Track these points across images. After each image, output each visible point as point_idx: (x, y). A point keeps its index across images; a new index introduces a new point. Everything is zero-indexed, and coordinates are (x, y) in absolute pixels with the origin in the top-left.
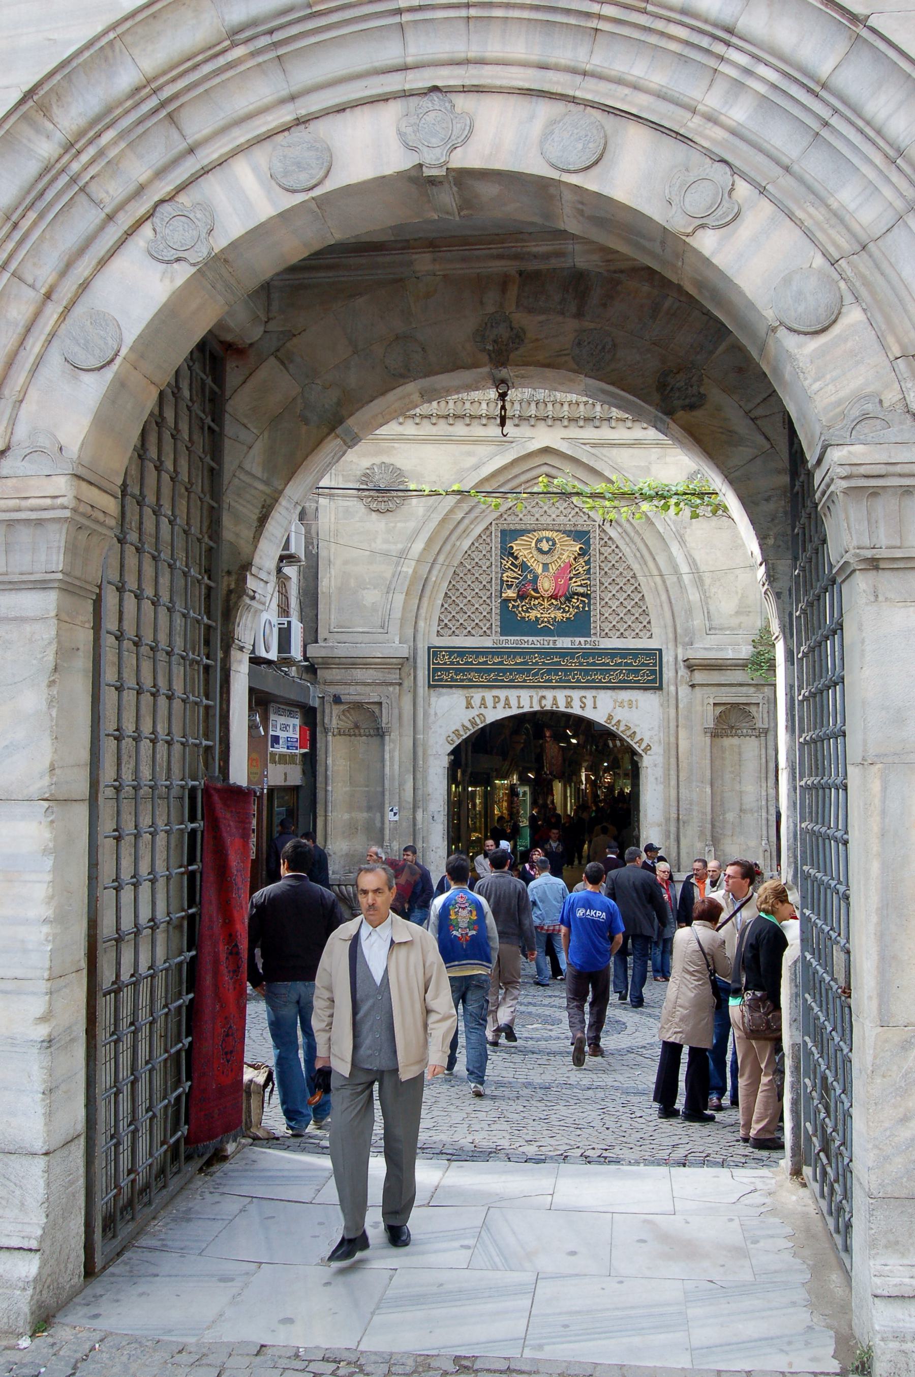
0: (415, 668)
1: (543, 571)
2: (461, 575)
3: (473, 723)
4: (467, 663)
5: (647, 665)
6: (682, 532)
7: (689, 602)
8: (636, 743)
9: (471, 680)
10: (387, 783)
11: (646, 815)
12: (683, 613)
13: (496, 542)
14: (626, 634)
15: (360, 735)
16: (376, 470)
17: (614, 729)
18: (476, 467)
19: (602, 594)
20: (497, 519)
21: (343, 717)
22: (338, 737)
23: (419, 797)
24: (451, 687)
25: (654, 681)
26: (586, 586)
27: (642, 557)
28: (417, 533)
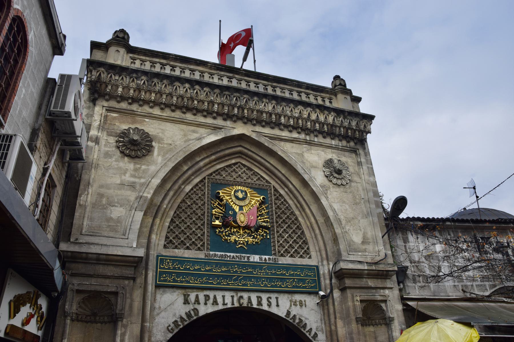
0: (147, 269)
1: (239, 211)
2: (184, 208)
3: (188, 315)
4: (185, 269)
7: (335, 233)
8: (307, 332)
12: (330, 242)
14: (295, 255)
16: (131, 131)
17: (291, 321)
18: (199, 139)
19: (279, 229)
21: (83, 306)
26: (267, 222)
27: (302, 206)
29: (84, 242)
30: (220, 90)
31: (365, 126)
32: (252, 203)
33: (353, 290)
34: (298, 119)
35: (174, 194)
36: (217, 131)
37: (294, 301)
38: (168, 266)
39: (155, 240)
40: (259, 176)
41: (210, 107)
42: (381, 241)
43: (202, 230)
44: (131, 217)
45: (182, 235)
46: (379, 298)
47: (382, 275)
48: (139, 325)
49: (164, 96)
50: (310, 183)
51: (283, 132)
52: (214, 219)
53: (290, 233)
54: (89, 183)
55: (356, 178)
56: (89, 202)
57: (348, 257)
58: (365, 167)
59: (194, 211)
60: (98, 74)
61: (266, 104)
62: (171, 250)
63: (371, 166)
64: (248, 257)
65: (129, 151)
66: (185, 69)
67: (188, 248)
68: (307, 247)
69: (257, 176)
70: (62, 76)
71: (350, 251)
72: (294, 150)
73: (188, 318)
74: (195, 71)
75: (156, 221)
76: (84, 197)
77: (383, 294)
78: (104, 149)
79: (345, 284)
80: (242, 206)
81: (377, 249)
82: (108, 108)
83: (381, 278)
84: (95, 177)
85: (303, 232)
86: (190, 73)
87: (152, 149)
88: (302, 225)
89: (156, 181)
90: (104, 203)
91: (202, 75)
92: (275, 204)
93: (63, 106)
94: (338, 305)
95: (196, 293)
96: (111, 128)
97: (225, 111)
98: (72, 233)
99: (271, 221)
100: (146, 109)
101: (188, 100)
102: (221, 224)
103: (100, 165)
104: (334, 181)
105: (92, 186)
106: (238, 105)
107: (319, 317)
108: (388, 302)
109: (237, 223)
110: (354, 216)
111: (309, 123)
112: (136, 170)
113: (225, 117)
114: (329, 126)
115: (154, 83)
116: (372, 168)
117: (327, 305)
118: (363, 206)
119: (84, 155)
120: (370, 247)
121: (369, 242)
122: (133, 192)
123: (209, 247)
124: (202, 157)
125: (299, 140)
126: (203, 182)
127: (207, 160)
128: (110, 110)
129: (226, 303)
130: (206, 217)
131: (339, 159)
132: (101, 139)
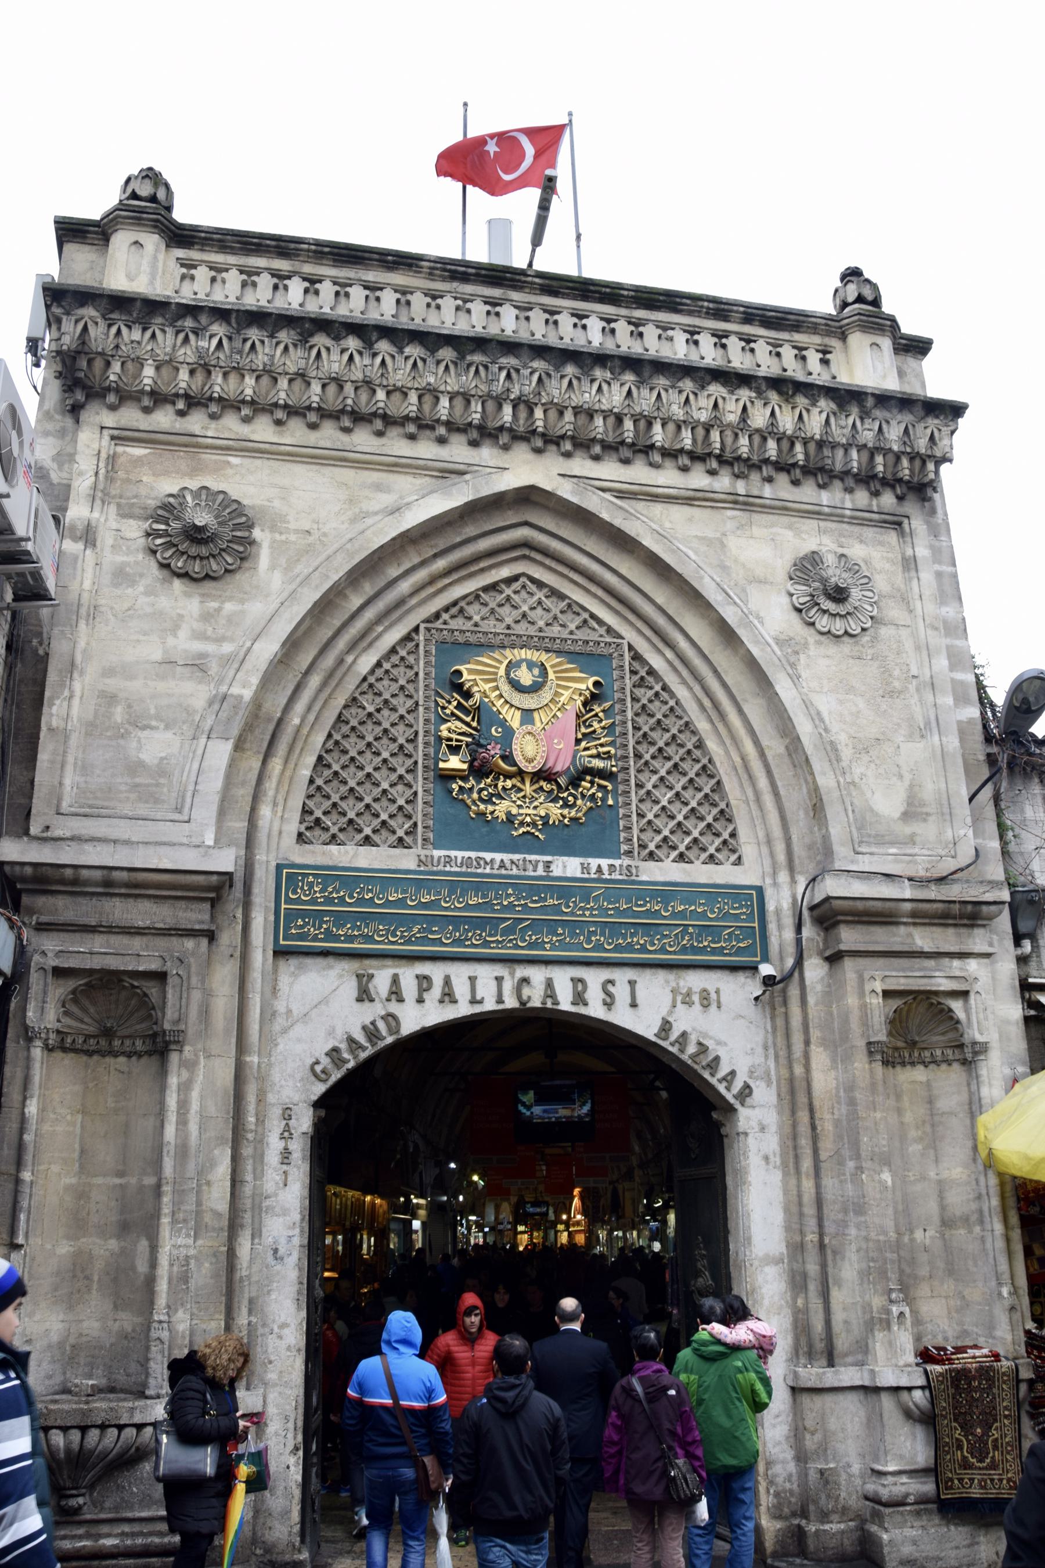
0: (247, 905)
1: (522, 724)
2: (354, 722)
3: (371, 1033)
4: (361, 902)
6: (792, 659)
7: (816, 789)
8: (720, 1081)
11: (749, 1240)
12: (802, 814)
14: (691, 854)
15: (115, 1055)
16: (189, 498)
17: (674, 1050)
18: (395, 511)
19: (642, 777)
20: (427, 621)
21: (74, 1009)
22: (58, 1055)
24: (325, 953)
26: (608, 756)
27: (716, 705)
29: (68, 834)
30: (455, 349)
31: (932, 438)
32: (562, 699)
33: (862, 962)
34: (708, 428)
35: (324, 684)
36: (449, 482)
37: (684, 991)
39: (271, 822)
41: (427, 408)
42: (963, 810)
43: (409, 786)
45: (351, 801)
46: (945, 985)
47: (962, 916)
48: (231, 1062)
49: (283, 383)
50: (741, 632)
51: (660, 472)
52: (445, 754)
53: (678, 787)
54: (73, 664)
55: (894, 612)
56: (75, 720)
57: (852, 862)
58: (927, 576)
59: (386, 731)
61: (605, 387)
62: (319, 848)
63: (950, 569)
64: (547, 865)
66: (351, 285)
67: (367, 841)
68: (730, 829)
69: (578, 614)
71: (861, 842)
72: (695, 531)
73: (370, 1040)
74: (381, 289)
76: (61, 706)
77: (958, 973)
78: (111, 559)
79: (839, 941)
81: (949, 834)
82: (116, 433)
83: (955, 925)
84: (88, 644)
85: (719, 783)
86: (367, 297)
87: (254, 549)
88: (718, 764)
89: (268, 648)
90: (119, 720)
91: (403, 300)
92: (635, 699)
94: (816, 1004)
96: (129, 494)
97: (474, 416)
98: (33, 811)
99: (620, 753)
100: (231, 425)
101: (356, 389)
103: (102, 609)
104: (823, 623)
105: (82, 673)
106: (512, 397)
107: (759, 1038)
108: (972, 996)
109: (515, 764)
110: (883, 733)
111: (744, 441)
112: (207, 617)
113: (474, 434)
114: (812, 447)
115: (248, 344)
116: (955, 576)
117: (785, 1003)
118: (913, 702)
119: (51, 584)
120: (927, 830)
121: (927, 814)
122: (200, 683)
123: (431, 835)
124: (407, 565)
125: (712, 495)
126: (412, 640)
127: (422, 575)
129: (478, 998)
130: (421, 747)
131: (840, 551)
132: (101, 528)
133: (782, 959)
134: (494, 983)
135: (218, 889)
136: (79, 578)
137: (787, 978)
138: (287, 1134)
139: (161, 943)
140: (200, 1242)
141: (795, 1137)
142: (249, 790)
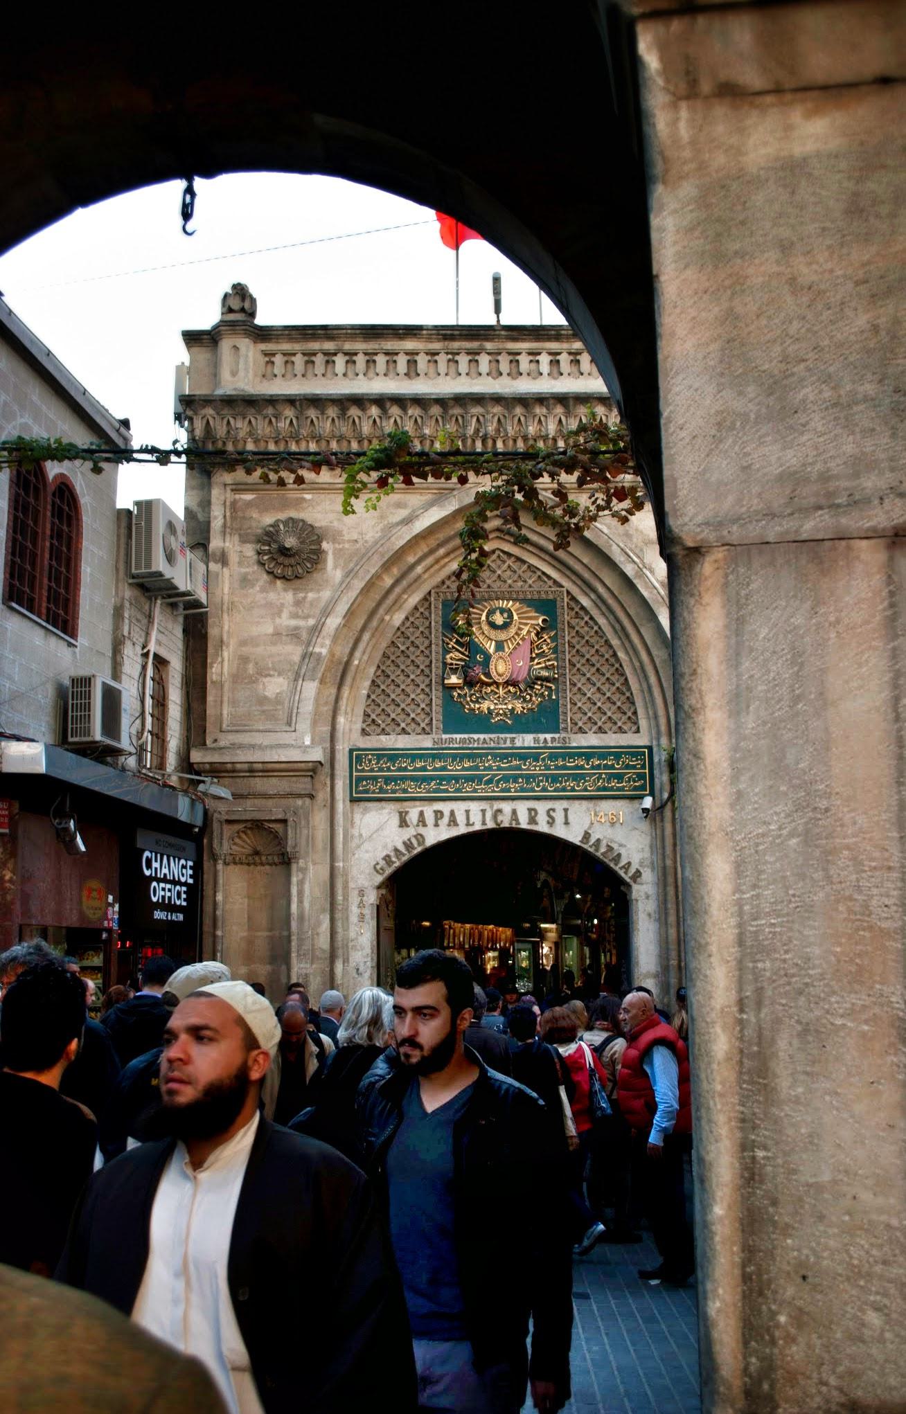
2: (393, 658)
3: (409, 845)
4: (400, 769)
5: (634, 767)
9: (405, 791)
10: (294, 925)
13: (436, 618)
15: (262, 864)
16: (282, 527)
17: (591, 850)
18: (408, 521)
21: (237, 840)
22: (232, 867)
23: (339, 943)
24: (380, 800)
25: (643, 788)
27: (623, 629)
28: (334, 602)
29: (228, 744)
38: (370, 767)
40: (539, 573)
44: (298, 693)
48: (328, 867)
50: (637, 582)
54: (222, 641)
60: (205, 422)
64: (513, 740)
65: (283, 570)
67: (404, 731)
68: (632, 710)
70: (138, 504)
75: (343, 691)
80: (502, 642)
82: (234, 487)
85: (626, 679)
86: (388, 361)
88: (625, 667)
93: (148, 564)
95: (420, 809)
96: (245, 527)
102: (460, 681)
105: (229, 643)
106: (481, 434)
109: (491, 678)
112: (298, 603)
117: (662, 820)
119: (204, 601)
124: (420, 554)
127: (430, 560)
128: (238, 488)
130: (434, 670)
133: (661, 793)
134: (480, 813)
135: (314, 770)
136: (220, 586)
137: (663, 806)
138: (361, 905)
139: (284, 802)
140: (314, 966)
141: (665, 901)
142: (331, 707)
